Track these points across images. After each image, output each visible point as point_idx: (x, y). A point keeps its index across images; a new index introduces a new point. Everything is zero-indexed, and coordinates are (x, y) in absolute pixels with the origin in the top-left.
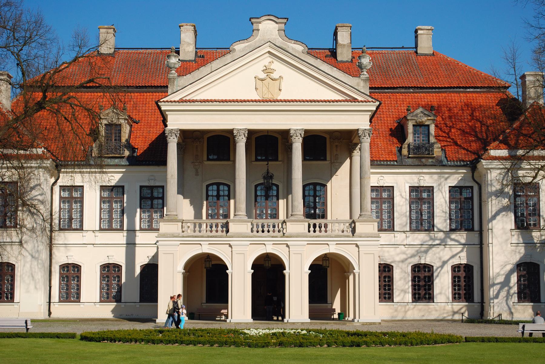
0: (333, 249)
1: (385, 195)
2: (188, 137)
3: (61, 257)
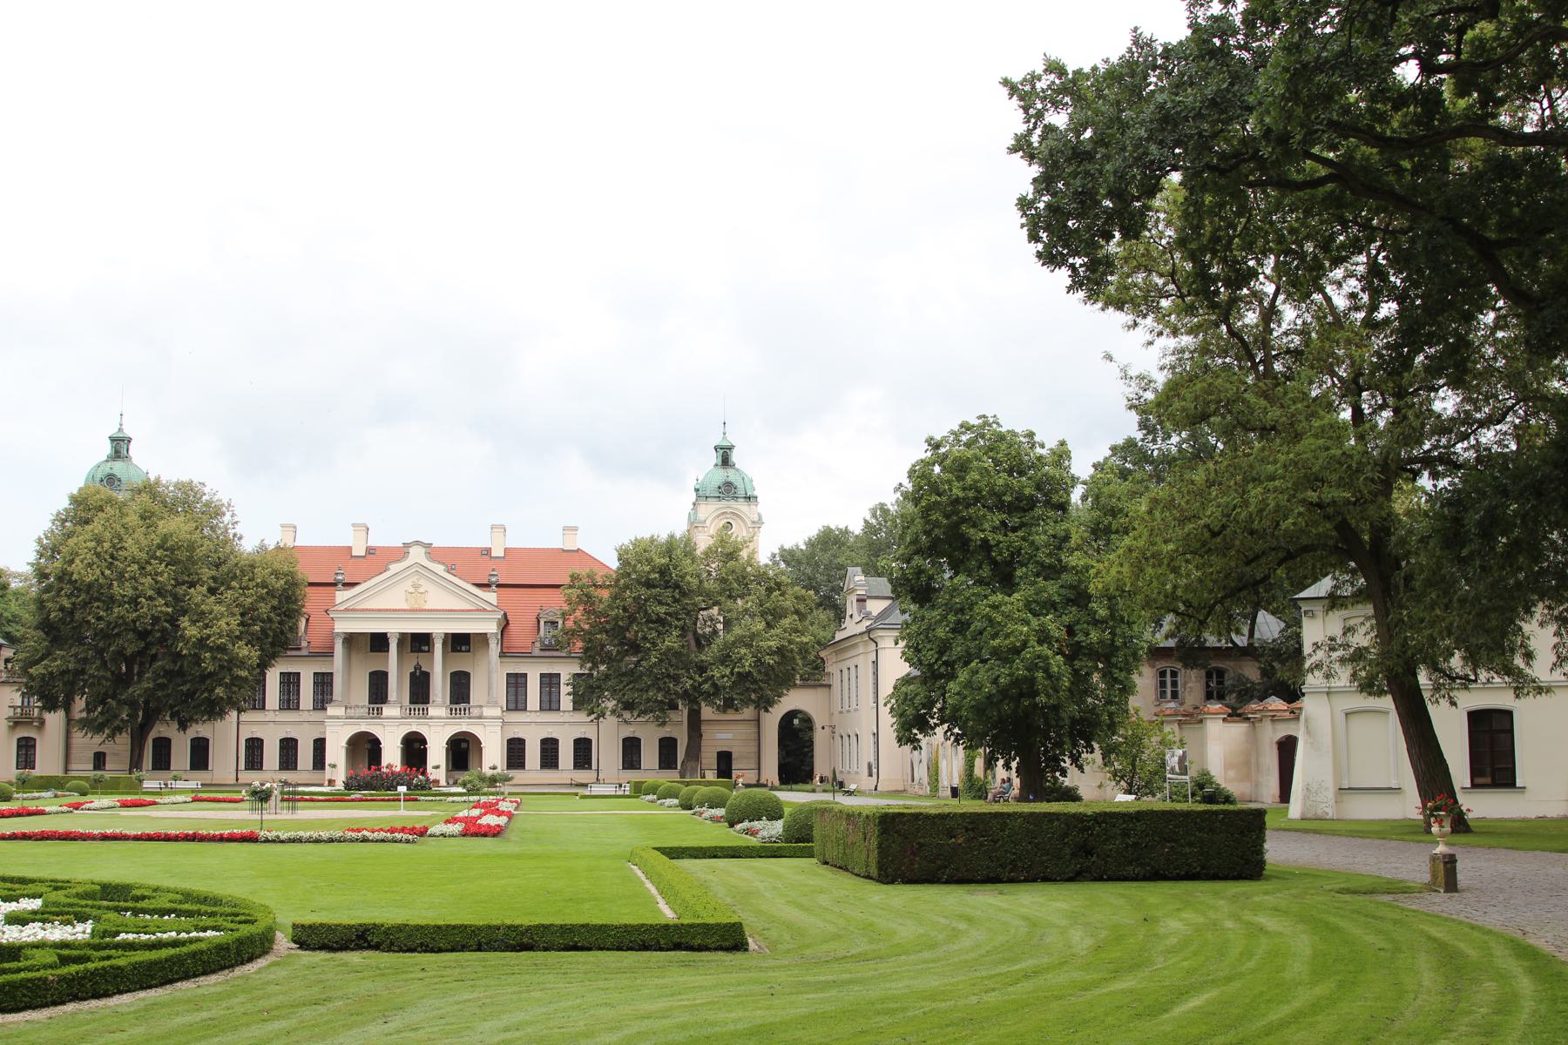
0: (464, 729)
1: (521, 680)
2: (351, 640)
3: (246, 733)
